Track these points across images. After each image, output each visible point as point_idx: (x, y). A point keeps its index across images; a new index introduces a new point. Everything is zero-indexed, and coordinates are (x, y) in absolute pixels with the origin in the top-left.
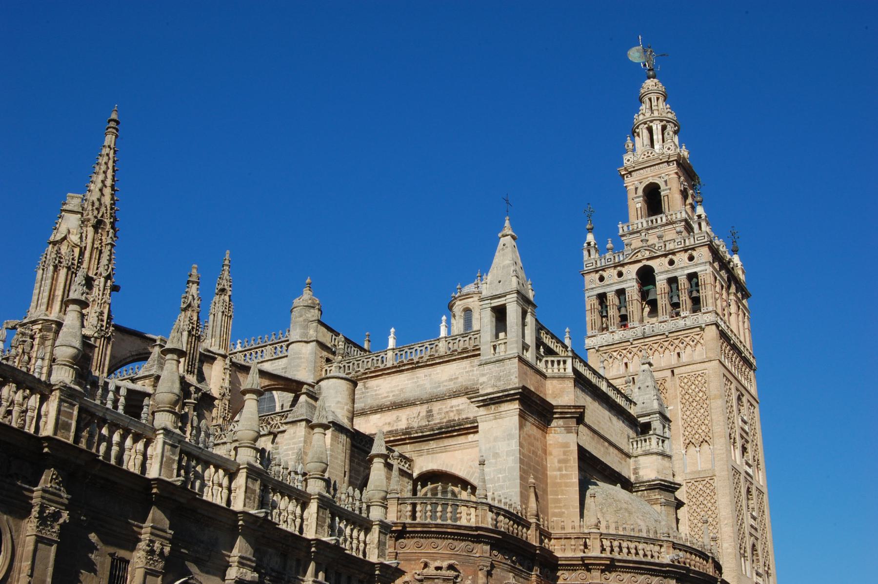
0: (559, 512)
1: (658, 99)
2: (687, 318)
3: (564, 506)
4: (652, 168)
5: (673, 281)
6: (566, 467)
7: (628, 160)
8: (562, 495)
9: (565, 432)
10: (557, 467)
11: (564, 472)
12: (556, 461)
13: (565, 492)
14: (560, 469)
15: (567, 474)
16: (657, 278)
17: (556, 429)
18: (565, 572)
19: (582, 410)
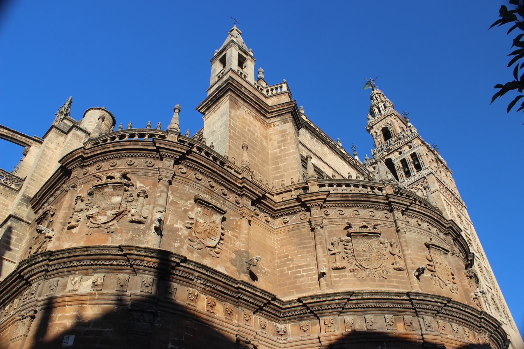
0: (280, 175)
1: (379, 96)
2: (416, 175)
3: (284, 170)
4: (382, 121)
5: (403, 161)
6: (283, 144)
7: (370, 123)
8: (281, 163)
9: (282, 123)
10: (277, 146)
11: (283, 148)
12: (276, 143)
13: (284, 161)
14: (279, 147)
15: (285, 149)
16: (394, 163)
17: (275, 123)
18: (286, 217)
19: (294, 105)
